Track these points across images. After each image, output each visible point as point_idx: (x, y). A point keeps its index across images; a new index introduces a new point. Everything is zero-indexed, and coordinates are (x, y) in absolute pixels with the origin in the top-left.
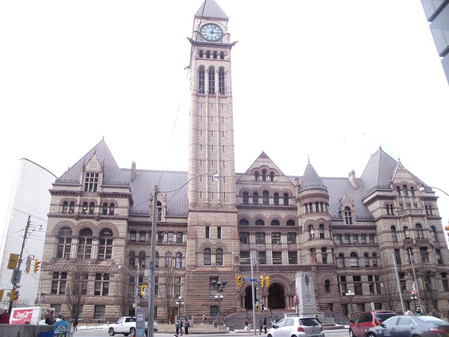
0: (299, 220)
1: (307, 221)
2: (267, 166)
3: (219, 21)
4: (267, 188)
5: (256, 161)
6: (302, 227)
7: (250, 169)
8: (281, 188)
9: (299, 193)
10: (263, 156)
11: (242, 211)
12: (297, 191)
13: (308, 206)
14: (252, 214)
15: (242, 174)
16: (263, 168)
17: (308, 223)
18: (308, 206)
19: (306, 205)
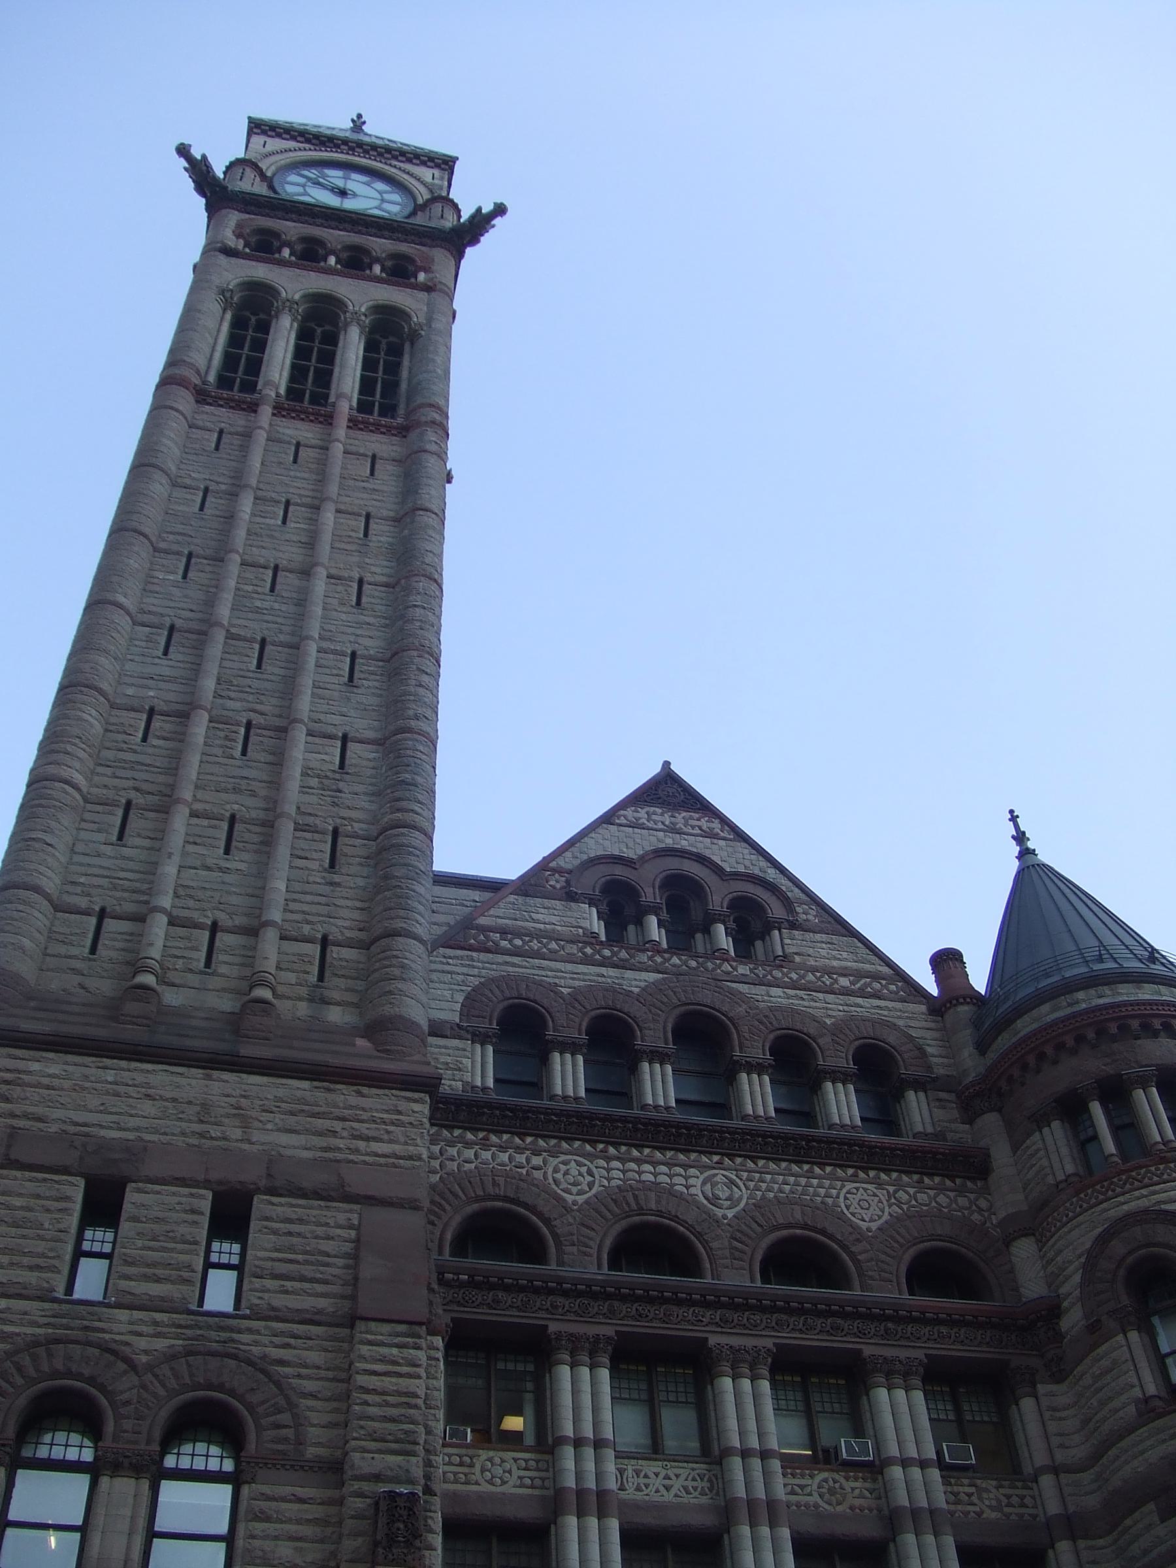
0: (1024, 1250)
1: (1103, 1240)
2: (701, 859)
3: (394, 163)
4: (707, 997)
5: (608, 819)
6: (1052, 1310)
7: (561, 862)
8: (826, 1009)
9: (982, 1047)
10: (667, 791)
11: (486, 1146)
12: (966, 1036)
13: (1096, 1108)
14: (576, 1179)
15: (493, 886)
16: (673, 864)
17: (1118, 1247)
18: (1096, 1108)
19: (1071, 1109)
